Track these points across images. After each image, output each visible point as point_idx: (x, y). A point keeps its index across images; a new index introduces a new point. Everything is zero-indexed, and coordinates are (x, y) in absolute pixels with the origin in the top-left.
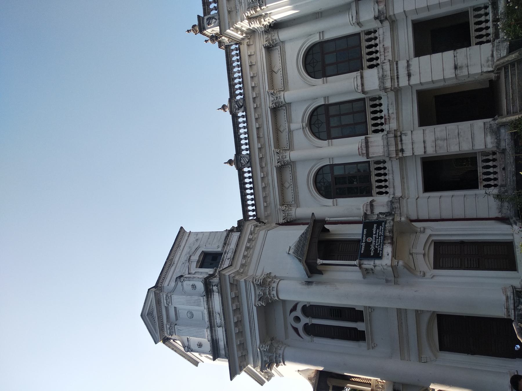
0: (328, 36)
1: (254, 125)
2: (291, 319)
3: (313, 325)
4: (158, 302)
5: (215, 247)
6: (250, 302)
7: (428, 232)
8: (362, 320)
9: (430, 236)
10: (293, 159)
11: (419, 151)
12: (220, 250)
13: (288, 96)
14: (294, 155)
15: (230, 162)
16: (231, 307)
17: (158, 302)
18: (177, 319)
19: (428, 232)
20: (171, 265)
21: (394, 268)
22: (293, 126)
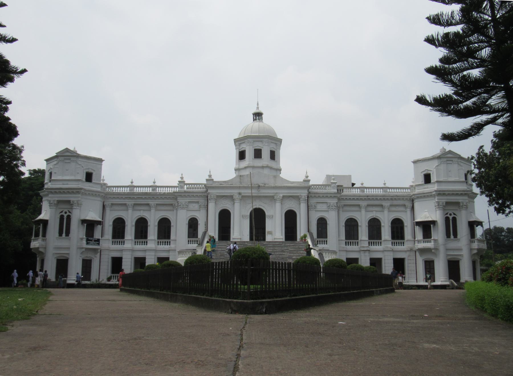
0: (172, 228)
1: (143, 197)
3: (63, 219)
7: (95, 258)
12: (93, 181)
13: (153, 211)
14: (130, 211)
15: (132, 183)
16: (70, 191)
19: (95, 258)
21: (83, 248)
22: (142, 211)
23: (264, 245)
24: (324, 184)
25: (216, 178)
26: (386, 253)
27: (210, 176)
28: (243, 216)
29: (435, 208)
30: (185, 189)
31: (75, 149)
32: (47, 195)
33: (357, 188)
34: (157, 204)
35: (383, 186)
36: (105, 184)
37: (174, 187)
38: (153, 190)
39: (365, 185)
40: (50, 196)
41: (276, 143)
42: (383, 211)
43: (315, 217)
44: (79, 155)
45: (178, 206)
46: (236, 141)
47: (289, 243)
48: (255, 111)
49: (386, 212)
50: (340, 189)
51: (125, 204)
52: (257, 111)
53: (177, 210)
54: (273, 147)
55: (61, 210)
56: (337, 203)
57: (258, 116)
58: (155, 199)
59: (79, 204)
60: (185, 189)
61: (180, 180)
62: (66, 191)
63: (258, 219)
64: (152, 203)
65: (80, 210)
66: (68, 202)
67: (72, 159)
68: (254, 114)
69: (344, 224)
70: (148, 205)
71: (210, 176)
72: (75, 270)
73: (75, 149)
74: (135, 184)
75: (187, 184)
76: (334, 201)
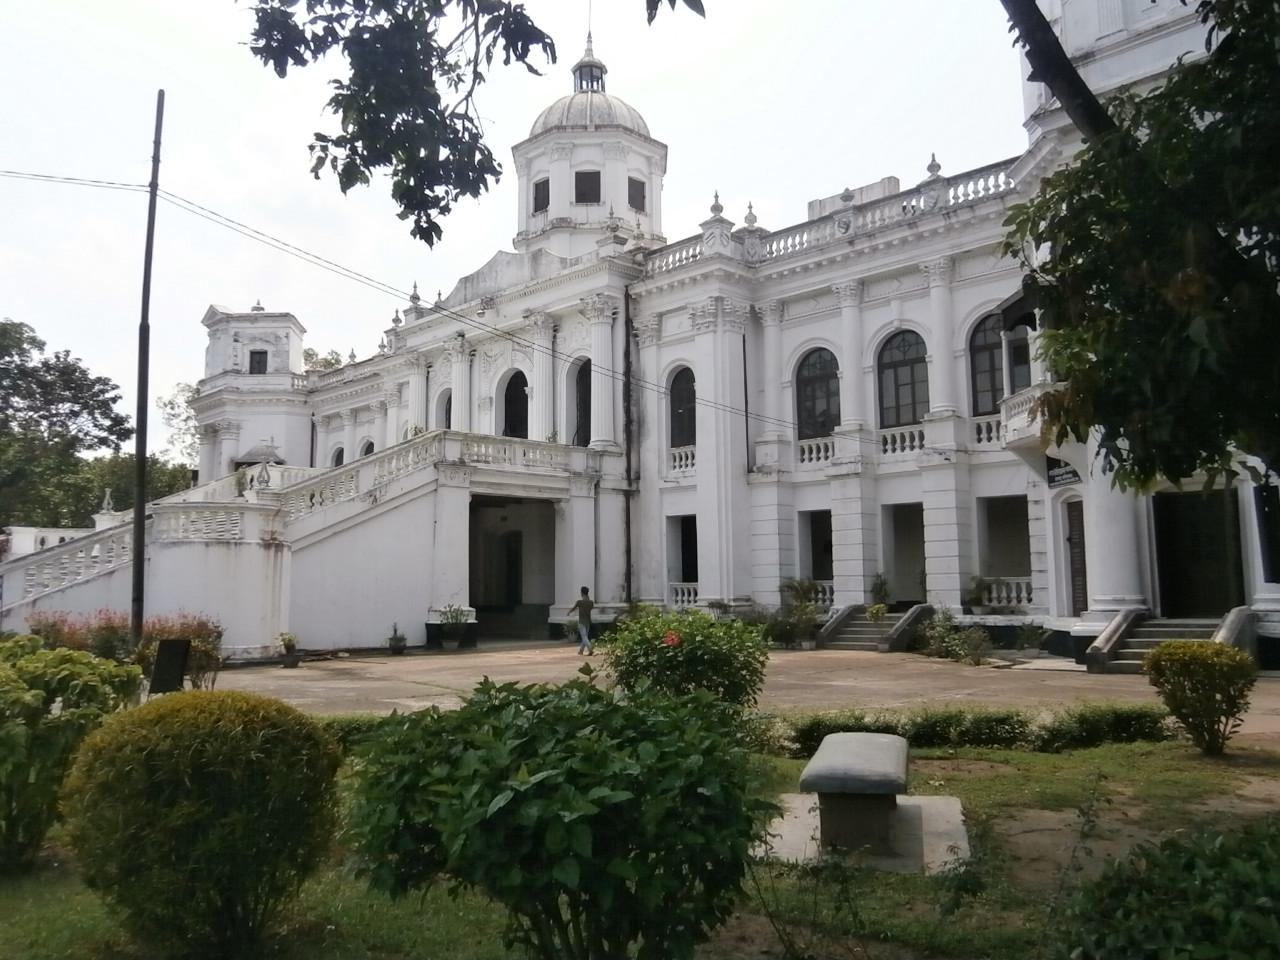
4: (220, 321)
5: (272, 363)
12: (270, 369)
17: (220, 321)
20: (252, 322)
26: (929, 481)
41: (601, 145)
49: (937, 293)
56: (719, 300)
59: (235, 428)
61: (391, 325)
65: (238, 440)
69: (789, 375)
74: (357, 360)
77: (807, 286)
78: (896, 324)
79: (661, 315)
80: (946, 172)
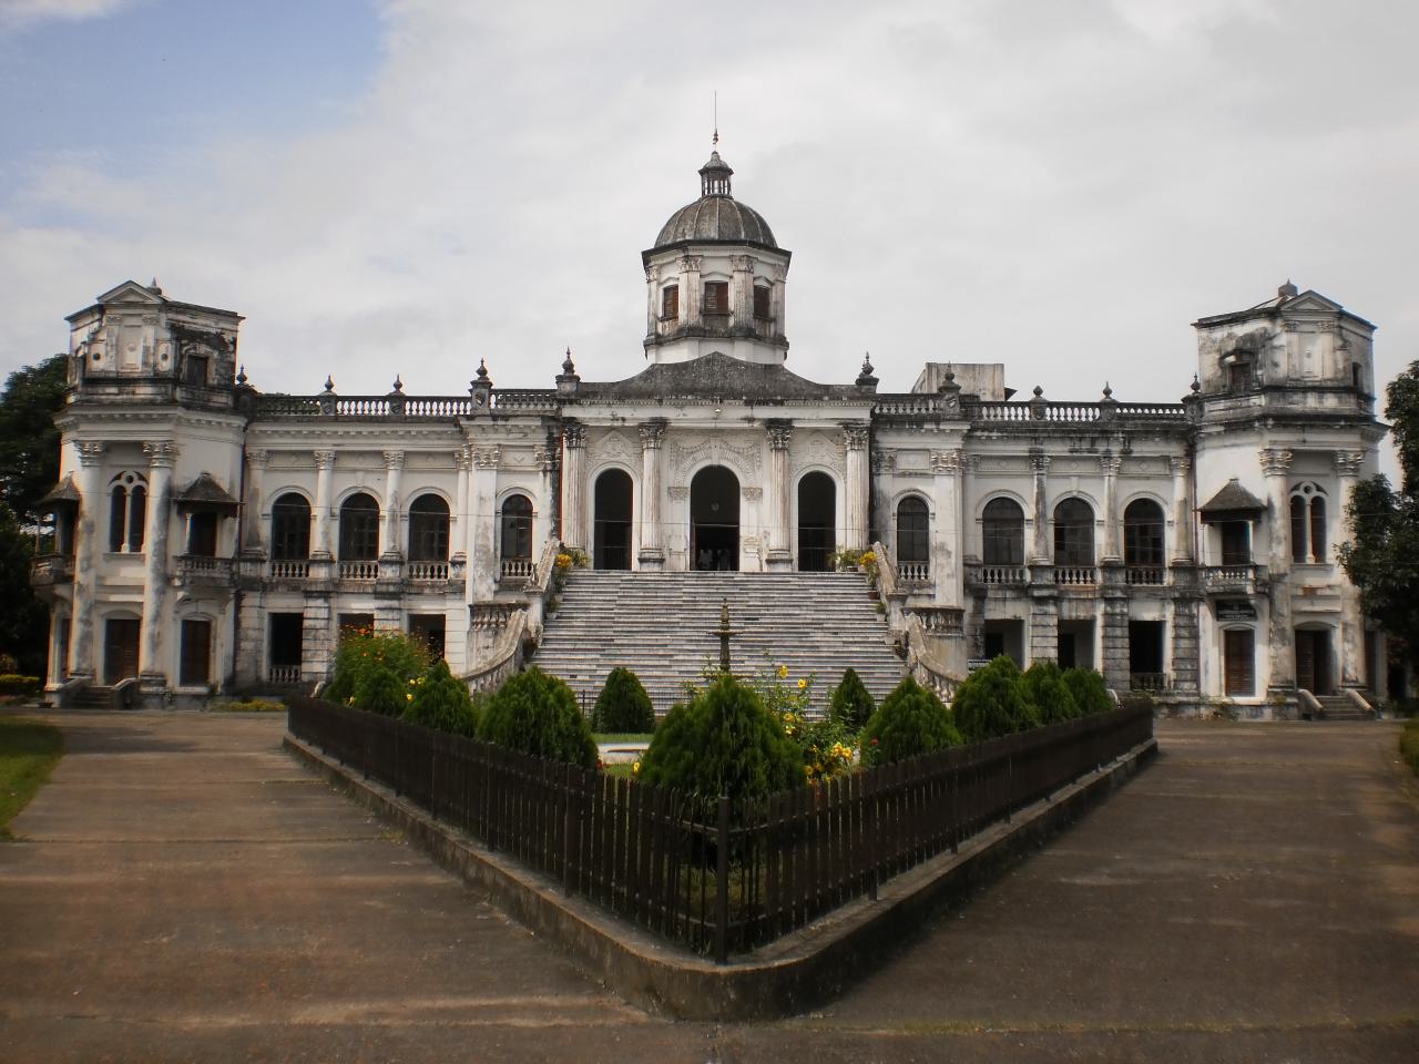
1: (365, 429)
2: (130, 472)
3: (125, 497)
6: (151, 434)
7: (220, 617)
8: (132, 550)
9: (216, 618)
10: (321, 472)
11: (309, 613)
18: (127, 326)
19: (220, 617)
22: (360, 475)
23: (736, 584)
24: (925, 391)
25: (587, 373)
27: (569, 367)
28: (674, 492)
29: (1261, 468)
30: (493, 406)
31: (154, 283)
32: (74, 426)
33: (1023, 405)
34: (406, 453)
35: (1099, 397)
36: (250, 391)
37: (459, 400)
38: (392, 409)
39: (1047, 396)
40: (83, 427)
41: (773, 266)
42: (1102, 478)
43: (893, 488)
44: (165, 301)
45: (470, 459)
46: (644, 253)
47: (812, 579)
48: (705, 160)
50: (970, 404)
51: (310, 453)
52: (714, 164)
53: (467, 470)
54: (763, 271)
55: (118, 471)
57: (716, 172)
58: (402, 437)
59: (170, 454)
60: (493, 406)
62: (129, 413)
63: (715, 502)
64: (393, 447)
66: (139, 445)
67: (149, 314)
68: (702, 172)
70: (380, 454)
71: (569, 367)
72: (158, 654)
73: (154, 283)
74: (338, 391)
75: (496, 392)
76: (949, 446)
77: (1005, 451)
78: (1075, 494)
79: (899, 450)
80: (1116, 396)
